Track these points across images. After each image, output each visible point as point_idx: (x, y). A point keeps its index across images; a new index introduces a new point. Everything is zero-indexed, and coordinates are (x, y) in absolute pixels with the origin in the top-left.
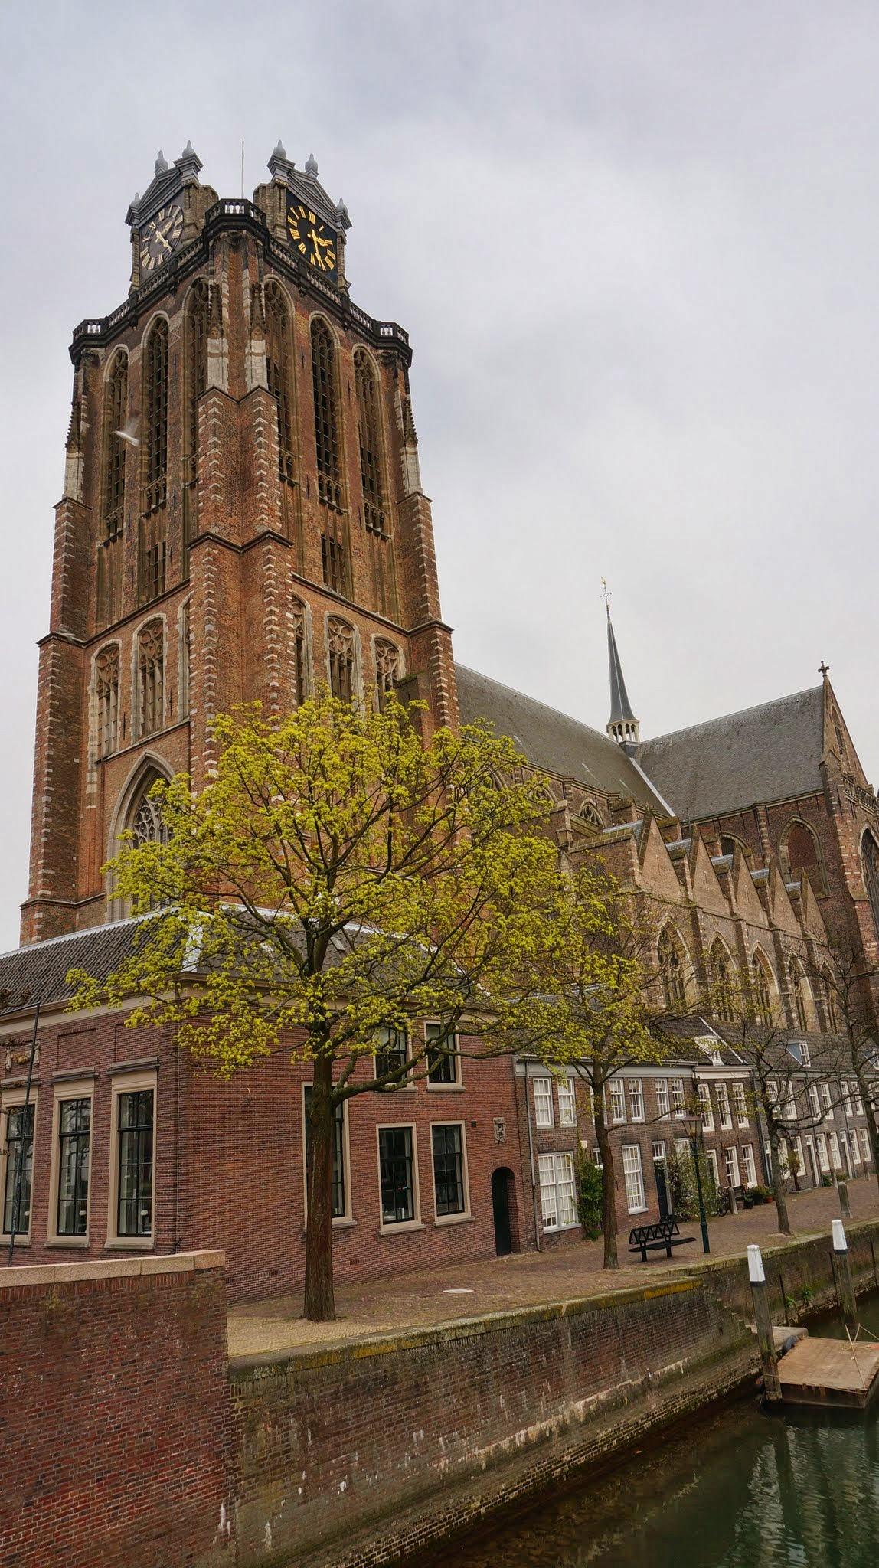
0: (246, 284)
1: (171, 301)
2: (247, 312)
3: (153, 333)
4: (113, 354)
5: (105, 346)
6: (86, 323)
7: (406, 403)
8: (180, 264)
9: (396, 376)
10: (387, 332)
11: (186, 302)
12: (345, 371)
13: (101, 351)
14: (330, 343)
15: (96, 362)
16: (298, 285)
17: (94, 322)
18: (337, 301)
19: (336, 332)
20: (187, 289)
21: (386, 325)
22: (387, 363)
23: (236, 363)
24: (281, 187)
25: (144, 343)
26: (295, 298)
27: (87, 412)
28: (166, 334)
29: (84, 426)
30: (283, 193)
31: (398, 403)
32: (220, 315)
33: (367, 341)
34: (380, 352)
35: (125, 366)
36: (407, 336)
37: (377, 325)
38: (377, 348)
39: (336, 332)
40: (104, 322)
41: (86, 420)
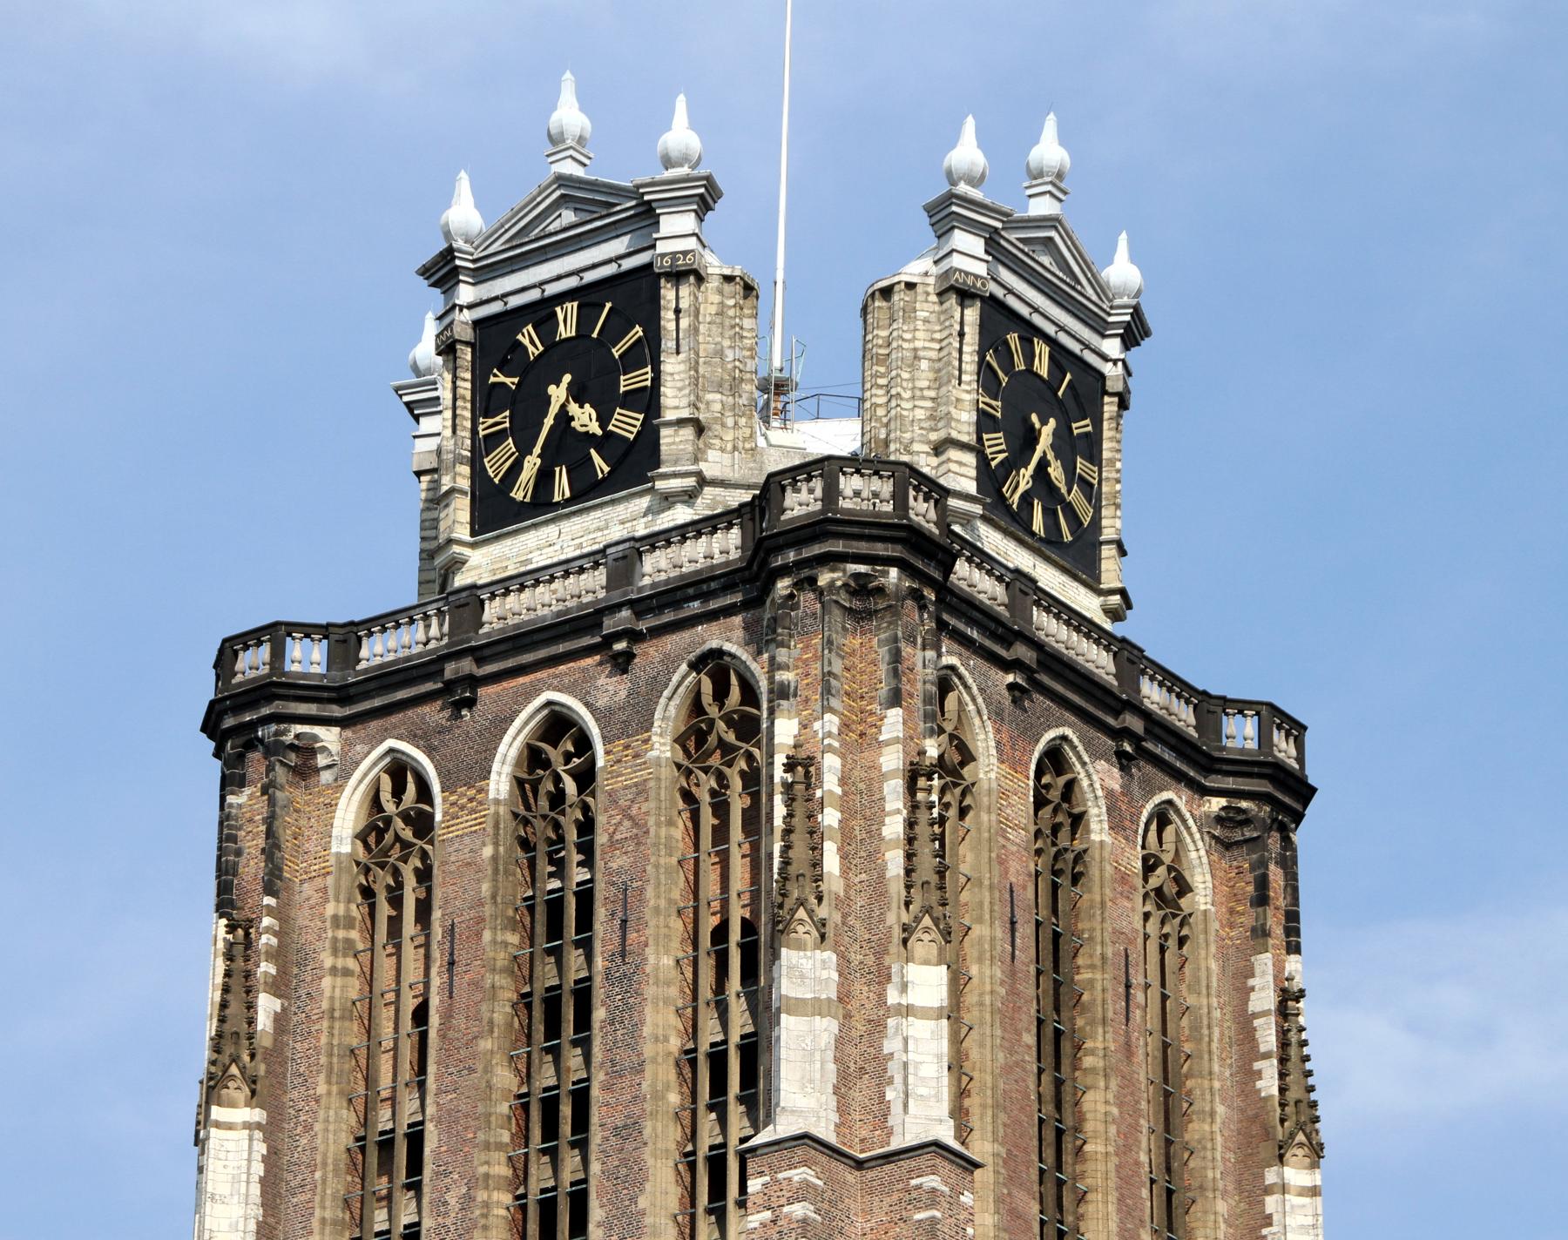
0: (892, 760)
1: (612, 689)
2: (895, 862)
3: (534, 758)
4: (369, 765)
5: (343, 723)
6: (276, 633)
7: (1288, 998)
8: (657, 568)
9: (1261, 899)
10: (1241, 733)
11: (668, 715)
12: (1114, 916)
13: (329, 737)
14: (1078, 820)
15: (304, 760)
16: (1006, 666)
17: (309, 630)
18: (1099, 662)
19: (1098, 778)
20: (670, 658)
21: (1241, 706)
22: (1229, 833)
23: (860, 1027)
24: (965, 295)
25: (500, 783)
26: (998, 715)
27: (276, 955)
28: (586, 778)
29: (267, 1006)
30: (972, 314)
31: (1264, 999)
32: (817, 864)
33: (1179, 777)
34: (1216, 804)
35: (422, 824)
36: (1295, 730)
37: (1210, 706)
38: (1205, 792)
39: (1098, 778)
40: (344, 638)
41: (278, 987)
